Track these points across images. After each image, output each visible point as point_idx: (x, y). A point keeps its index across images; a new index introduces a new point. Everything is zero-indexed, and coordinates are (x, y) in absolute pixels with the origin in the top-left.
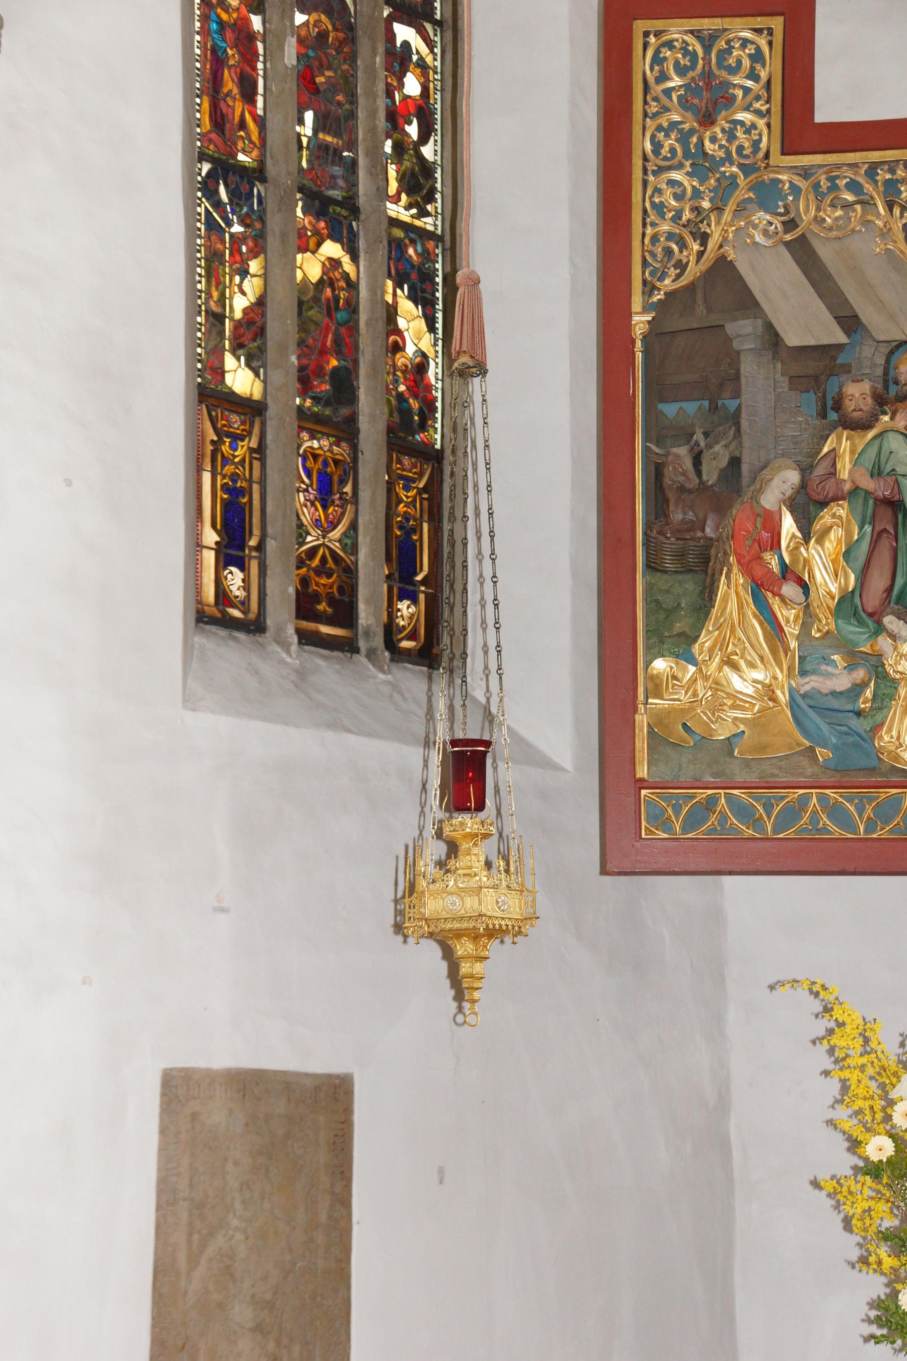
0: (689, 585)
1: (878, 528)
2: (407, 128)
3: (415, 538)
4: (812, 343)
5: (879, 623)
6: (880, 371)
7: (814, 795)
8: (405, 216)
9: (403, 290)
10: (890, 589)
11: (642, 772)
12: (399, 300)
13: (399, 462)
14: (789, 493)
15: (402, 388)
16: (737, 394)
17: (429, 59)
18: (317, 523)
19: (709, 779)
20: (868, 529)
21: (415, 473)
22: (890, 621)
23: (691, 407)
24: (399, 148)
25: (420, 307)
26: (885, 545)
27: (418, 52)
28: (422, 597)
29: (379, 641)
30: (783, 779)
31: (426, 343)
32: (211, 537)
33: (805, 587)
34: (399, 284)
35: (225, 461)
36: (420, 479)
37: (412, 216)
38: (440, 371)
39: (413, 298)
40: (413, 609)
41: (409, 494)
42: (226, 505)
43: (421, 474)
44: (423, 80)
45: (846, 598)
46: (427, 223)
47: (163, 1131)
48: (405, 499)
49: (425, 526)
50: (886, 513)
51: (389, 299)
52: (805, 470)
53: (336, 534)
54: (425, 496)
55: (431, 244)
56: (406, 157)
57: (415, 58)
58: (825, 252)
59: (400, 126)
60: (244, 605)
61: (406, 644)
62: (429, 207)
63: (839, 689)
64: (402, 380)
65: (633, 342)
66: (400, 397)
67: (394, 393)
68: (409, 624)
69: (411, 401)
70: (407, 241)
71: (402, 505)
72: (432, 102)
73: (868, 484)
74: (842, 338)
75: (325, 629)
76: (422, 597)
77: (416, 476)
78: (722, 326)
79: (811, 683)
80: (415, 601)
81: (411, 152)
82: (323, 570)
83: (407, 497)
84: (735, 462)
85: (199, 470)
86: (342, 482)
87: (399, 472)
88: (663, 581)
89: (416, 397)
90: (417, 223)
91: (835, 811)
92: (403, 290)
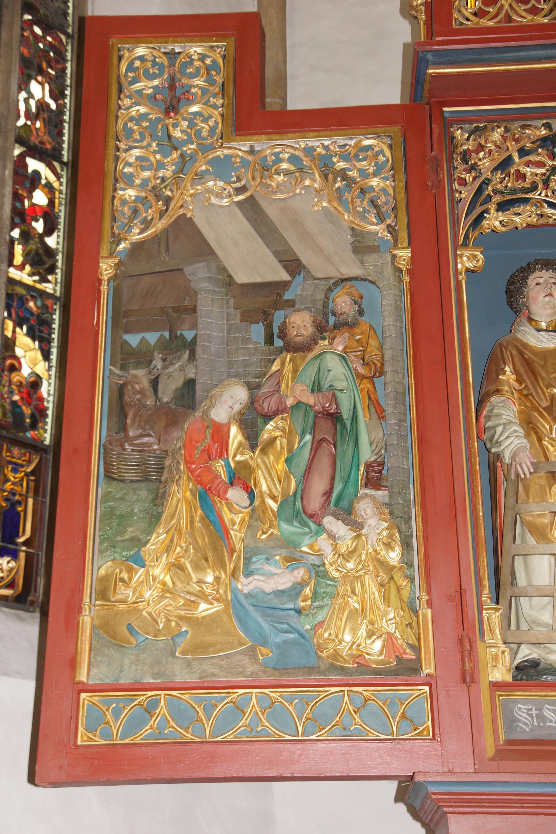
1: (318, 438)
2: (34, 224)
3: (20, 509)
4: (258, 279)
5: (320, 525)
6: (320, 305)
7: (254, 695)
8: (29, 280)
9: (22, 328)
10: (328, 494)
12: (17, 335)
13: (9, 450)
14: (237, 408)
15: (16, 398)
16: (194, 326)
17: (56, 185)
19: (149, 680)
20: (308, 437)
21: (24, 461)
22: (329, 521)
23: (152, 338)
24: (26, 236)
25: (37, 343)
27: (46, 178)
28: (22, 555)
30: (223, 678)
31: (41, 368)
34: (19, 323)
36: (28, 466)
37: (35, 281)
38: (52, 389)
39: (31, 334)
40: (13, 564)
41: (17, 476)
43: (30, 462)
44: (49, 196)
46: (48, 288)
48: (12, 479)
49: (30, 501)
50: (325, 425)
51: (9, 334)
52: (252, 388)
54: (33, 478)
55: (49, 302)
56: (31, 242)
57: (43, 182)
58: (271, 211)
59: (28, 221)
62: (50, 277)
63: (281, 587)
64: (16, 392)
65: (100, 281)
66: (14, 403)
67: (8, 401)
68: (8, 576)
69: (24, 408)
70: (29, 297)
71: (9, 484)
72: (56, 210)
74: (285, 277)
76: (22, 555)
77: (24, 463)
78: (182, 270)
81: (37, 240)
83: (15, 478)
84: (190, 384)
87: (9, 458)
89: (29, 404)
90: (38, 286)
92: (22, 328)
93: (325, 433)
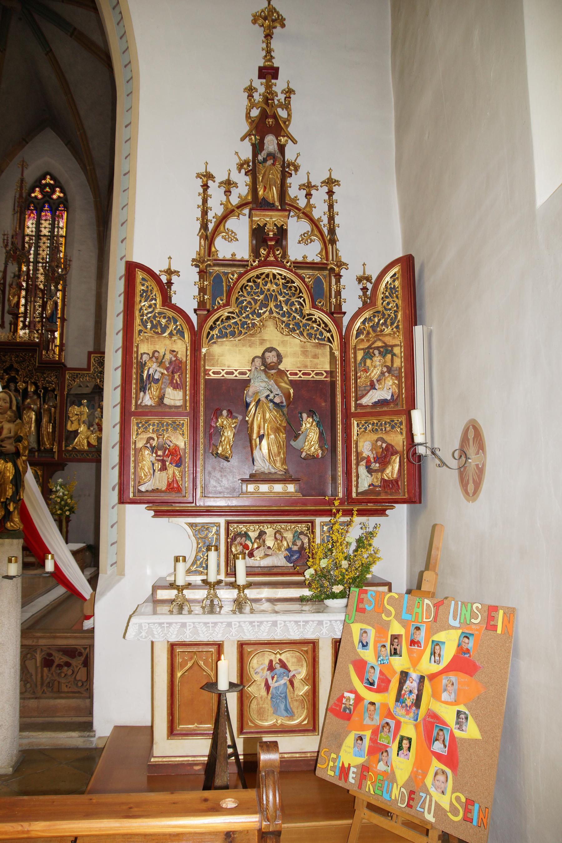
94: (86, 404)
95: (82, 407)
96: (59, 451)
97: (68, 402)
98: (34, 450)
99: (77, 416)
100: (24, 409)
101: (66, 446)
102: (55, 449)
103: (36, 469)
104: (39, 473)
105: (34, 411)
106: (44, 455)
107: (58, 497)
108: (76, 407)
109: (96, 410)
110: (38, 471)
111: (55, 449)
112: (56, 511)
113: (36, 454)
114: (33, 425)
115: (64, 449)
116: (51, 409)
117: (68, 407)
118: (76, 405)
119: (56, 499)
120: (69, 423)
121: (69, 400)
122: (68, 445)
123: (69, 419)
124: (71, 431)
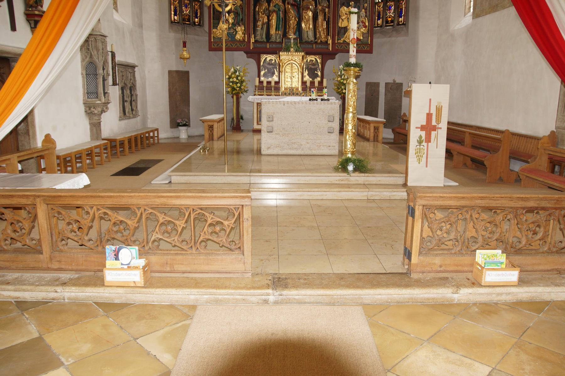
0: (217, 21)
11: (212, 41)
18: (185, 11)
22: (237, 25)
26: (236, 18)
29: (193, 24)
32: (173, 13)
33: (229, 22)
35: (175, 4)
42: (174, 9)
45: (233, 23)
47: (169, 76)
53: (188, 11)
60: (177, 20)
61: (197, 24)
73: (235, 11)
75: (187, 23)
79: (230, 31)
80: (198, 19)
82: (186, 16)
85: (171, 5)
86: (188, 5)
88: (214, 21)
91: (232, 45)
93: (236, 15)
94: (353, 5)
95: (350, 8)
96: (332, 44)
97: (339, 4)
98: (312, 42)
99: (346, 16)
100: (303, 10)
101: (338, 40)
102: (330, 42)
103: (316, 57)
104: (319, 61)
105: (312, 11)
106: (320, 46)
107: (344, 79)
108: (345, 8)
109: (361, 11)
110: (318, 59)
111: (330, 42)
112: (342, 90)
113: (314, 46)
114: (311, 22)
115: (336, 42)
116: (325, 10)
117: (339, 8)
118: (345, 6)
119: (342, 81)
120: (341, 20)
121: (339, 2)
122: (339, 39)
123: (340, 17)
124: (342, 28)
